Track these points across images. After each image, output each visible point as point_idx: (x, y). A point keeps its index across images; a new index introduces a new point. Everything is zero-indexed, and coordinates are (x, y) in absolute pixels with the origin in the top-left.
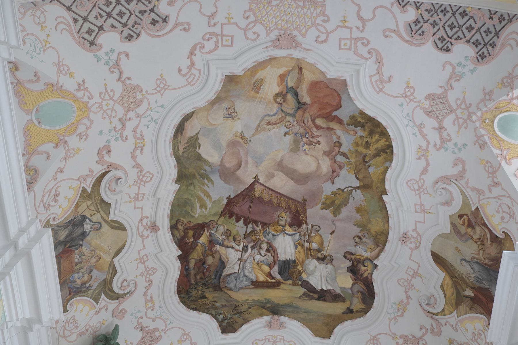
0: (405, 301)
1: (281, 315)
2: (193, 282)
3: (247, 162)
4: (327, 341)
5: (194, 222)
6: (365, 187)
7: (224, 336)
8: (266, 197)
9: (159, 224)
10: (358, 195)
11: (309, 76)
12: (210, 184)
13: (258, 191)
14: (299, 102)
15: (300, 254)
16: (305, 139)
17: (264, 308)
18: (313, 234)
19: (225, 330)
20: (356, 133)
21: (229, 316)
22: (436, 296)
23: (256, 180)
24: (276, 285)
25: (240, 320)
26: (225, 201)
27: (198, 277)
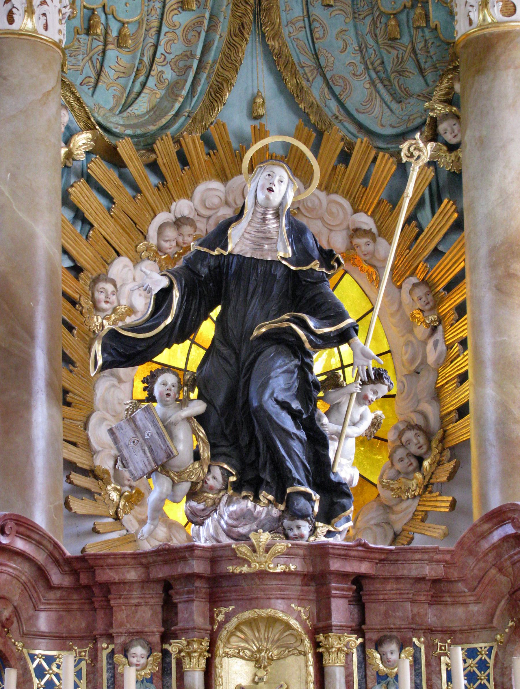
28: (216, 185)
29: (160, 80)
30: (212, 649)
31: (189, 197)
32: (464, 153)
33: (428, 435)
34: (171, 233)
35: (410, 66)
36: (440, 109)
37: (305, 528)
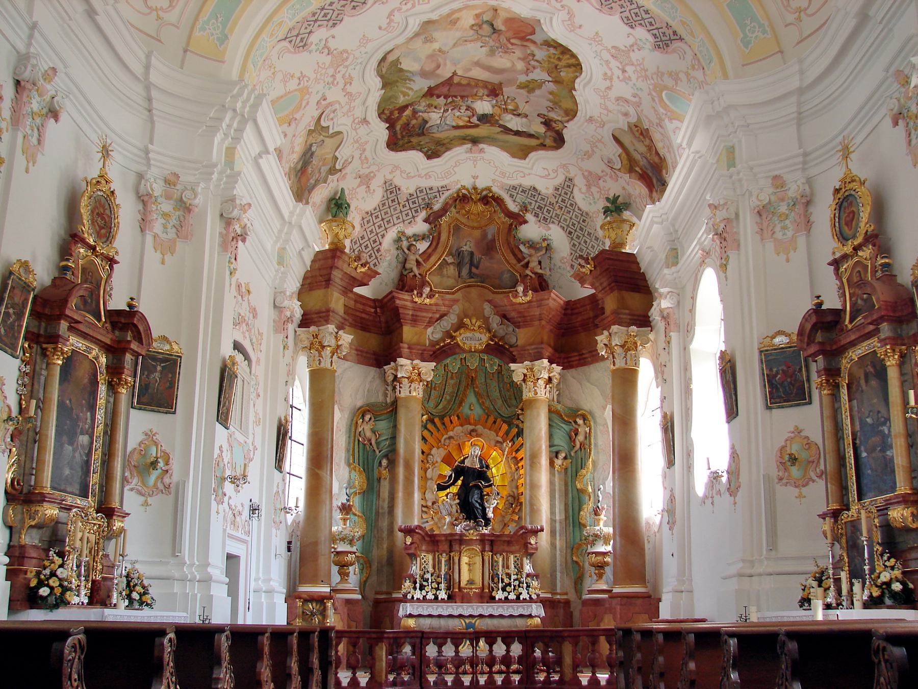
0: (590, 152)
1: (481, 143)
2: (400, 137)
3: (445, 64)
4: (523, 161)
5: (398, 106)
6: (556, 82)
7: (429, 161)
8: (464, 82)
9: (369, 118)
10: (551, 86)
11: (503, 15)
12: (412, 82)
13: (456, 80)
14: (494, 29)
15: (497, 111)
16: (500, 50)
17: (464, 139)
18: (509, 101)
19: (429, 157)
20: (549, 51)
21: (433, 148)
22: (614, 160)
23: (455, 74)
24: (476, 126)
25: (443, 149)
26: (426, 89)
27: (404, 133)
28: (460, 428)
29: (446, 399)
30: (460, 554)
31: (452, 430)
32: (525, 424)
33: (514, 497)
34: (448, 441)
35: (513, 397)
36: (520, 412)
37: (481, 528)
